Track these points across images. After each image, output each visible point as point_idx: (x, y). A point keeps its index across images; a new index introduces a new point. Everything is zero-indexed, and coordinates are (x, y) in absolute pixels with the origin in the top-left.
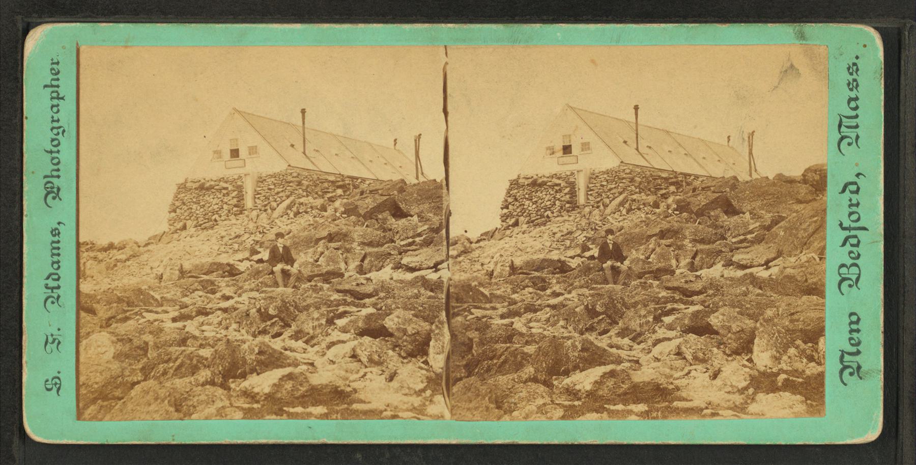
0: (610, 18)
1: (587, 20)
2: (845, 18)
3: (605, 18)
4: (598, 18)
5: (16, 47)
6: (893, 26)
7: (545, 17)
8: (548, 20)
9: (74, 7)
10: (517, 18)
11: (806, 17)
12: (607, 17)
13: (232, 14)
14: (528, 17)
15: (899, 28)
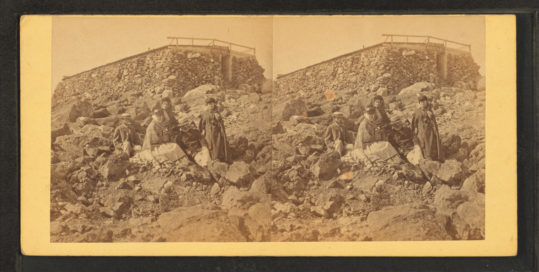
0: (362, 10)
1: (349, 11)
2: (501, 8)
3: (360, 10)
4: (356, 10)
5: (14, 32)
6: (528, 12)
7: (324, 10)
8: (326, 12)
9: (48, 7)
10: (307, 11)
11: (478, 8)
12: (361, 9)
13: (141, 11)
14: (314, 10)
15: (532, 14)
